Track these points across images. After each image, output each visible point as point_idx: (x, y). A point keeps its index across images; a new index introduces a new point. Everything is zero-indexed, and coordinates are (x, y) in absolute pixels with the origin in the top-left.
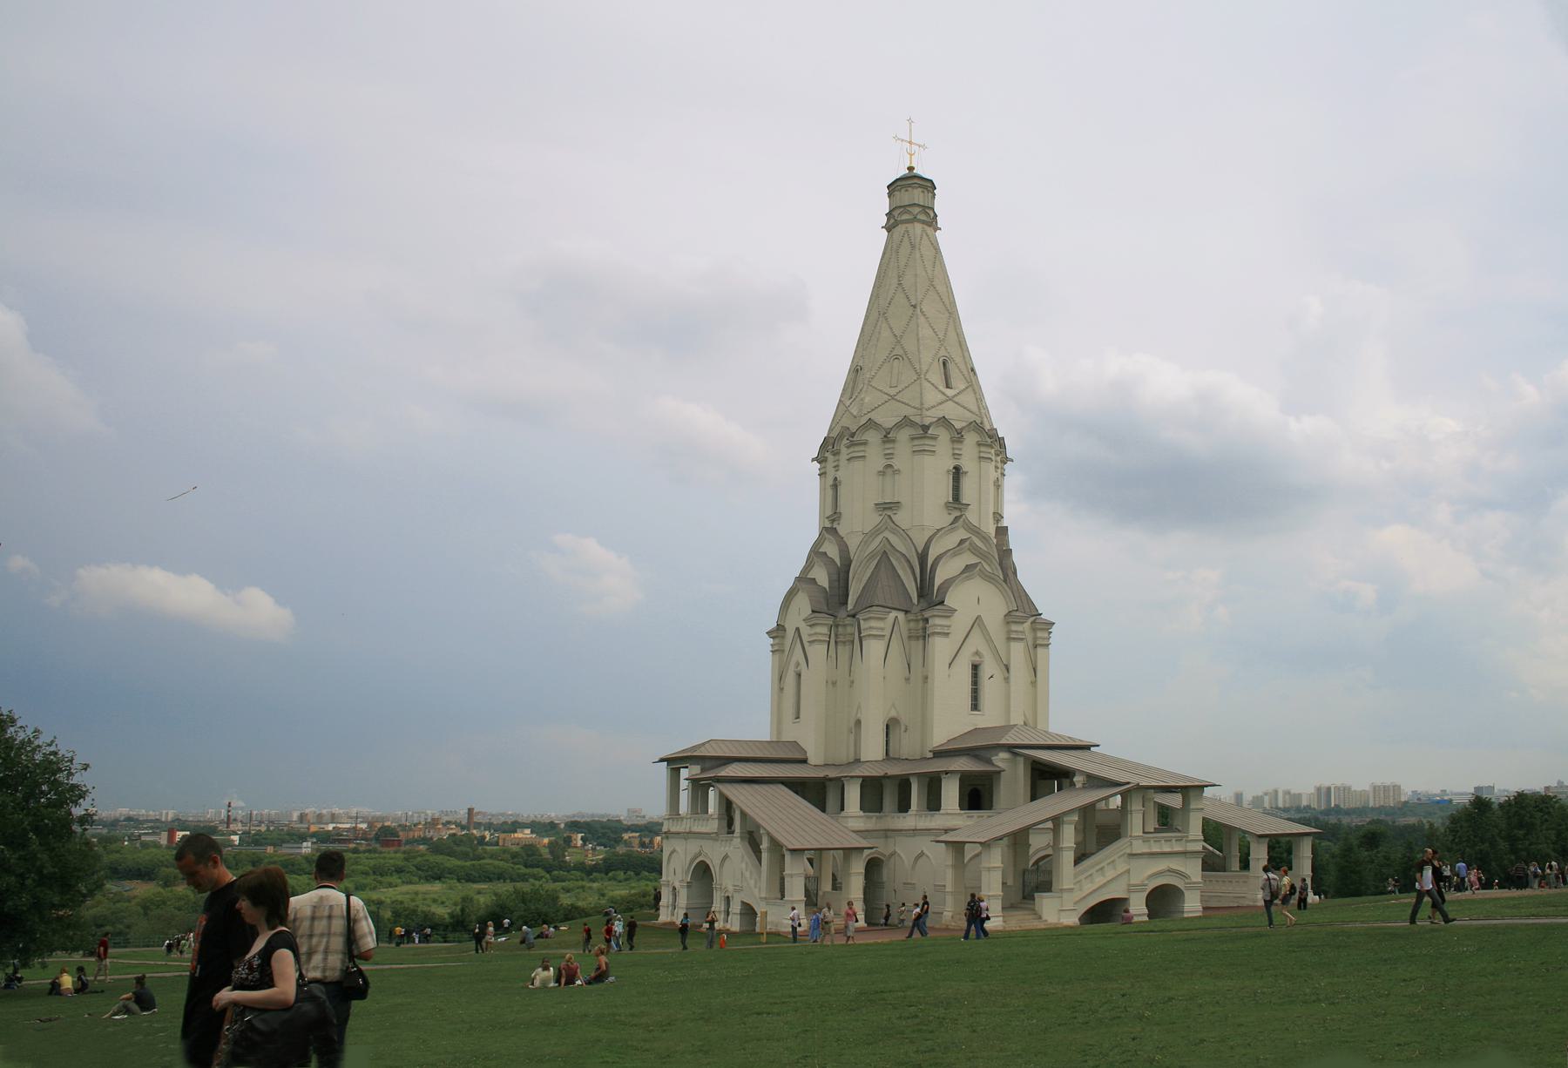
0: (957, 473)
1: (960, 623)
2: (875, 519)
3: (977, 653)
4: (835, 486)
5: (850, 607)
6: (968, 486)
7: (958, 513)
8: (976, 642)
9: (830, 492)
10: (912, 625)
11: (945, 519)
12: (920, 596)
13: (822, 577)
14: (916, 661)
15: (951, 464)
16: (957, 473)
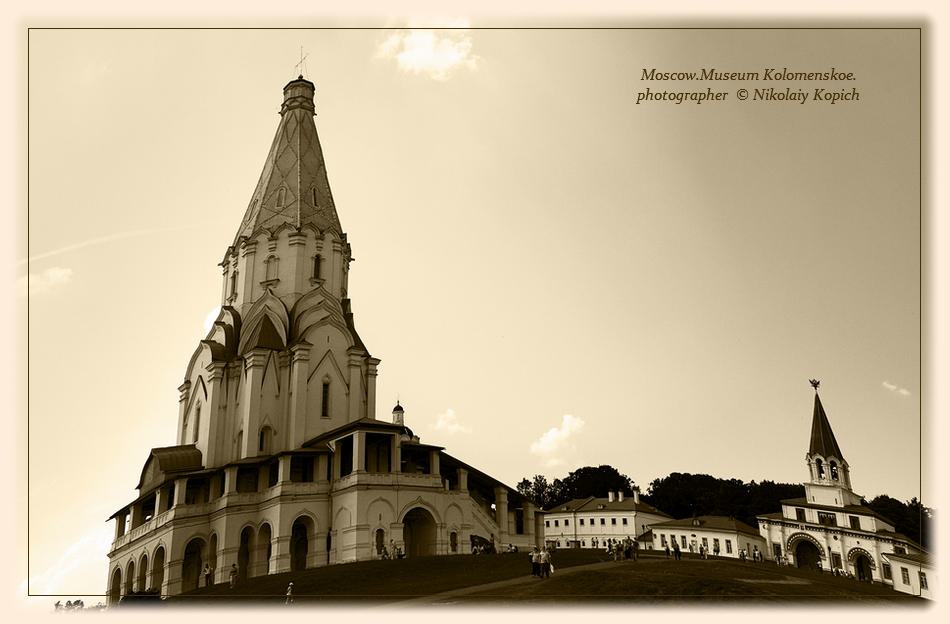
0: (318, 260)
1: (316, 357)
2: (259, 292)
3: (327, 376)
4: (234, 278)
5: (239, 354)
6: (325, 268)
7: (317, 286)
8: (328, 367)
9: (230, 281)
10: (283, 359)
11: (308, 288)
12: (288, 341)
13: (220, 337)
14: (284, 384)
15: (314, 252)
16: (318, 260)
